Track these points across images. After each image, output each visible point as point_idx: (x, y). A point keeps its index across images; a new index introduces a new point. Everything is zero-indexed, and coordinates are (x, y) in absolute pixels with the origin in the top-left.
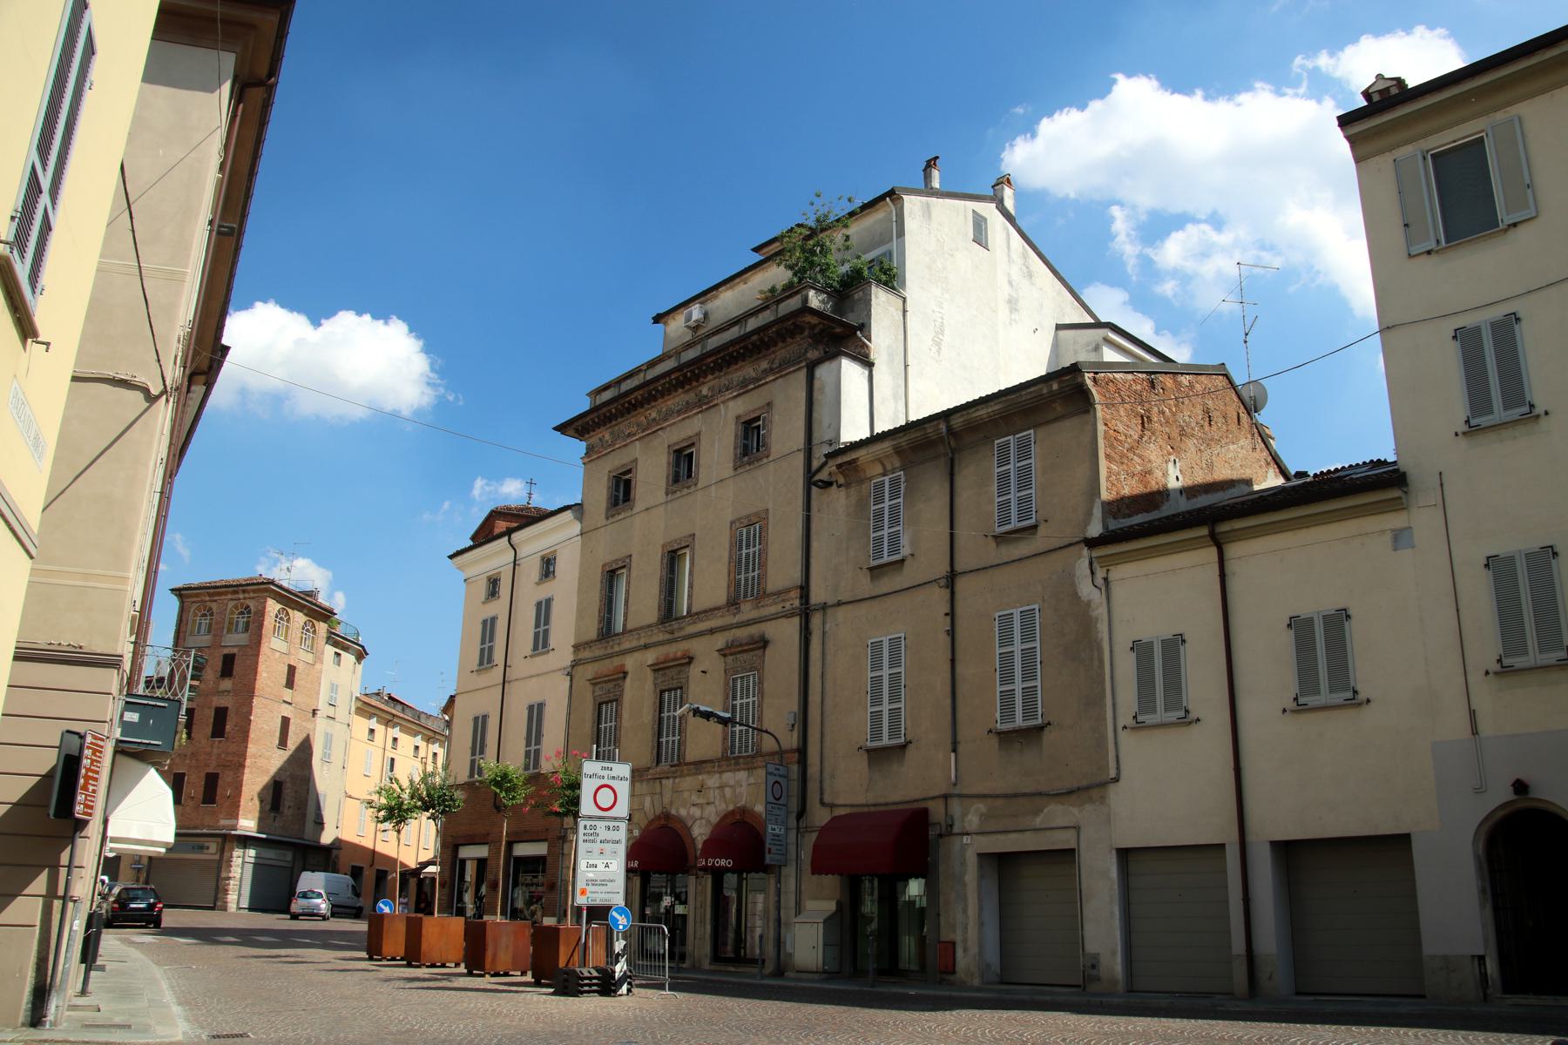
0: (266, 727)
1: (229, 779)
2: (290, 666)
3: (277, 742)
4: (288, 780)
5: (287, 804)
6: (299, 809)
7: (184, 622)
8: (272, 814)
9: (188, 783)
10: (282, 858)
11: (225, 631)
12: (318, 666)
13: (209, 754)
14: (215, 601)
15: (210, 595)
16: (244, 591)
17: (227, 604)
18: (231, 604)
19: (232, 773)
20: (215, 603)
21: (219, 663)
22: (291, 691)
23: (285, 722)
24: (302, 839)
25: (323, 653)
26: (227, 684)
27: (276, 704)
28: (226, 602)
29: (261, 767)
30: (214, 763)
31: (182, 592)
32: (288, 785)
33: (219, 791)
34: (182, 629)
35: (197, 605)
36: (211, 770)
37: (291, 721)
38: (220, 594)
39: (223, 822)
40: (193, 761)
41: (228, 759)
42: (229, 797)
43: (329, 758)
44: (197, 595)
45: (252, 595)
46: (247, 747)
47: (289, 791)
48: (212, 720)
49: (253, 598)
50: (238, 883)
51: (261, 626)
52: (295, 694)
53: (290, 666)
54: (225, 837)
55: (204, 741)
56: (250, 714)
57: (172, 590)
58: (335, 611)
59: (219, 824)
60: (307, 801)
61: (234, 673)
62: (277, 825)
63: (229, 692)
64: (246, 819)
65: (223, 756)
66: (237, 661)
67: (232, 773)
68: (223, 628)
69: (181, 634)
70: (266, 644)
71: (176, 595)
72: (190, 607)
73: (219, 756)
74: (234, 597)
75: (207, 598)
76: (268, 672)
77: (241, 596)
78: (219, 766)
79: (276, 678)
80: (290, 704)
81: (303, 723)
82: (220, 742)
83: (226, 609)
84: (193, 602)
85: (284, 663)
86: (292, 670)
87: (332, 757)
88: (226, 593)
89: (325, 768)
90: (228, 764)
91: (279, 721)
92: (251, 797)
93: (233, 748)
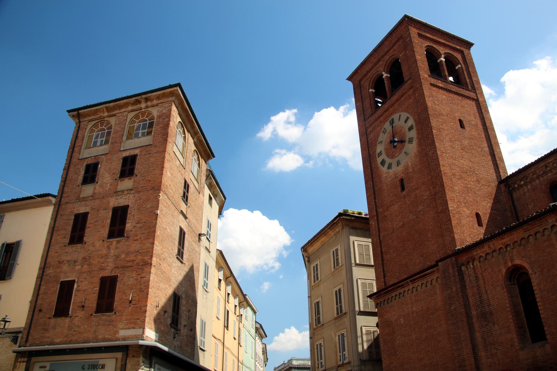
0: (168, 230)
1: (131, 281)
7: (79, 139)
9: (78, 290)
11: (125, 138)
14: (114, 115)
15: (108, 109)
16: (147, 100)
17: (127, 115)
19: (134, 274)
20: (114, 117)
21: (117, 166)
26: (127, 183)
27: (176, 212)
30: (111, 265)
31: (80, 112)
33: (118, 296)
34: (78, 144)
35: (93, 123)
36: (107, 273)
38: (120, 107)
39: (123, 333)
41: (128, 259)
42: (130, 302)
44: (96, 112)
45: (155, 102)
46: (154, 243)
49: (157, 105)
51: (167, 125)
54: (125, 349)
55: (98, 244)
56: (157, 208)
57: (69, 111)
59: (117, 336)
61: (136, 172)
65: (123, 256)
66: (137, 161)
68: (123, 135)
69: (76, 149)
71: (73, 116)
72: (87, 126)
73: (117, 257)
74: (134, 107)
75: (106, 114)
82: (118, 242)
83: (126, 120)
88: (126, 105)
90: (129, 264)
93: (135, 246)
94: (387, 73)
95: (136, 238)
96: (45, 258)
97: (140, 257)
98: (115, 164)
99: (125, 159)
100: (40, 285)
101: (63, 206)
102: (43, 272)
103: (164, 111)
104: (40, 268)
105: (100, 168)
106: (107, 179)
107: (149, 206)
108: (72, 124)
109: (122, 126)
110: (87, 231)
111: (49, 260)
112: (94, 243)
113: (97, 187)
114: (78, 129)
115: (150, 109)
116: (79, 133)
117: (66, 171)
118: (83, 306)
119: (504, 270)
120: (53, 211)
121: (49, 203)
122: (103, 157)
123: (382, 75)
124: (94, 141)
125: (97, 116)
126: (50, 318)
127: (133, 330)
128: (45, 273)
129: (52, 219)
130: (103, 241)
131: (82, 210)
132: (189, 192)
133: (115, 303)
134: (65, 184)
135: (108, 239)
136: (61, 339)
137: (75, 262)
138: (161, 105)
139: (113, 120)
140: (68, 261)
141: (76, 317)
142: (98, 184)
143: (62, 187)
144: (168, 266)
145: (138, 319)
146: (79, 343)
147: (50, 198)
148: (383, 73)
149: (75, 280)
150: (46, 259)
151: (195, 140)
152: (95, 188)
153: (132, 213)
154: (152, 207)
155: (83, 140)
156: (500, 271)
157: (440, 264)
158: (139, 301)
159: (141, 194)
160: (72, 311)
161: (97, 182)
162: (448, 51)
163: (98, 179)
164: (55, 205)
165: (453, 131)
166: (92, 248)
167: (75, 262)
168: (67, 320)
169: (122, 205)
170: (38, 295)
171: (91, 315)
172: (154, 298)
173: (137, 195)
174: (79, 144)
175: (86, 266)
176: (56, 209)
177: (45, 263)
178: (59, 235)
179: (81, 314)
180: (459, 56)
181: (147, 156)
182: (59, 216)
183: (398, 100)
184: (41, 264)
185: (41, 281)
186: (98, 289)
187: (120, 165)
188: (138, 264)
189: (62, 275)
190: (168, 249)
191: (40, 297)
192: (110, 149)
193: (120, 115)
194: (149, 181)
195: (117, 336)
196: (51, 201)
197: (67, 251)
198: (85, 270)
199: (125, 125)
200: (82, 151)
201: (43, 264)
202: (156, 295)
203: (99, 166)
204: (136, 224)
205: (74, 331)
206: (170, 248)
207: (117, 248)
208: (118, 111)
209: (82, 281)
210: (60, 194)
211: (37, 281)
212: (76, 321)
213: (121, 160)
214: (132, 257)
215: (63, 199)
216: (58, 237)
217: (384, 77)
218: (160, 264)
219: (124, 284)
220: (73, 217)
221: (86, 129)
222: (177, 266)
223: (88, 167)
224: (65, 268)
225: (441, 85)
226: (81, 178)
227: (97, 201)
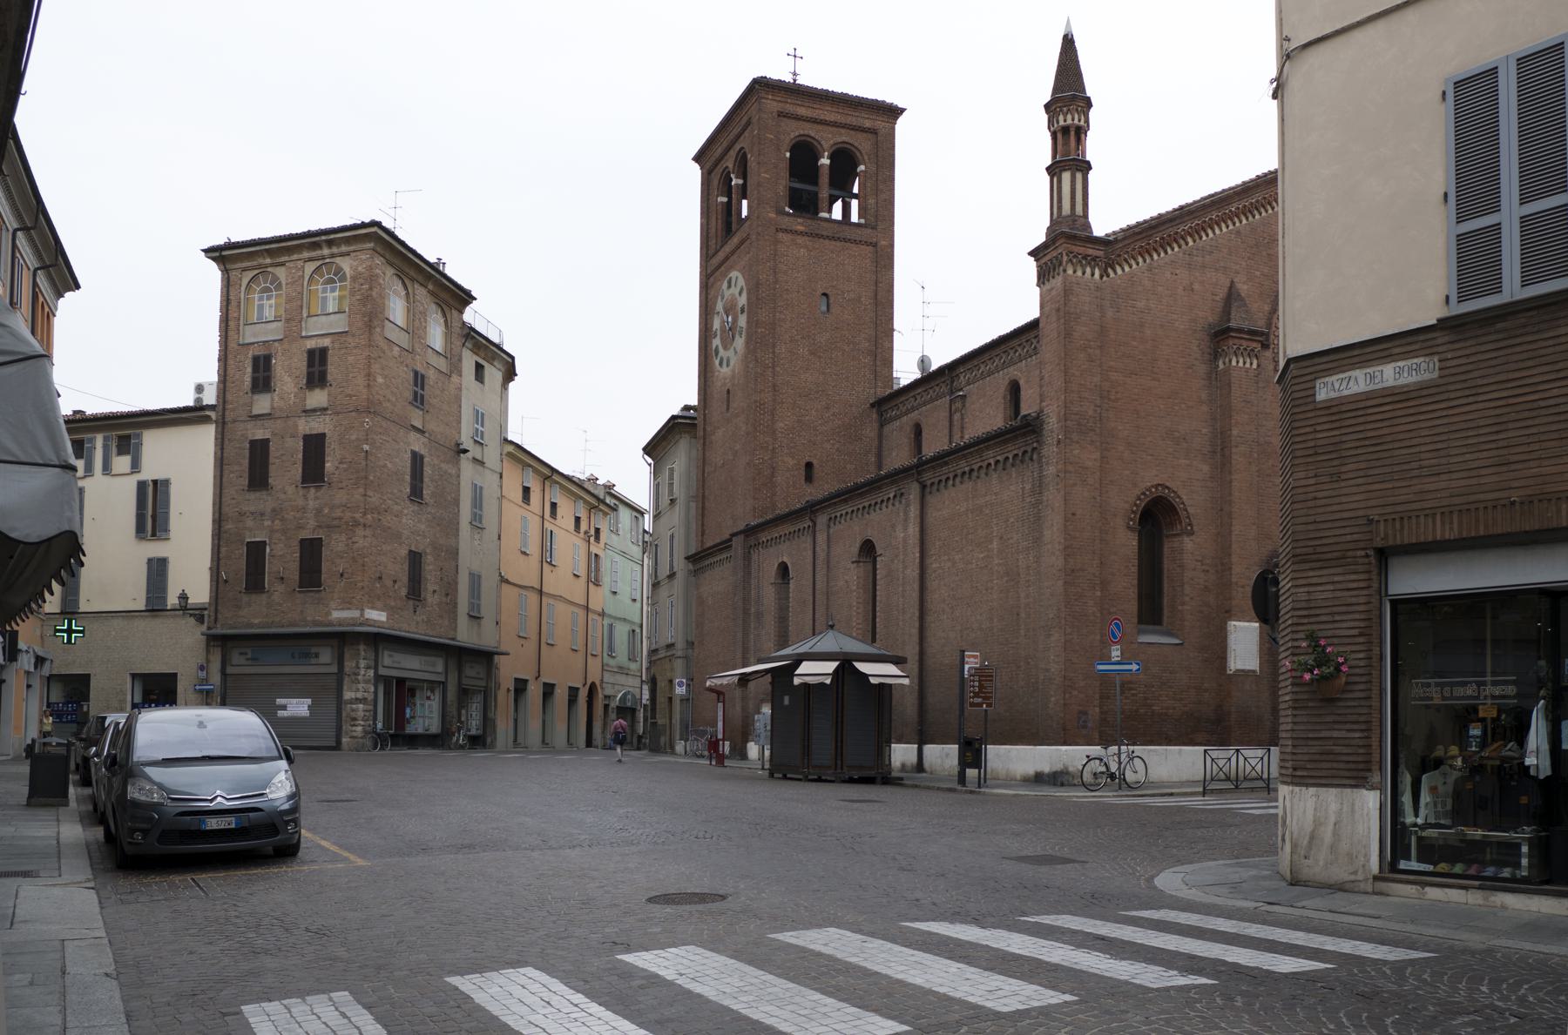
0: (389, 465)
1: (341, 547)
2: (416, 373)
3: (408, 490)
4: (428, 551)
5: (431, 588)
6: (447, 595)
7: (233, 304)
8: (411, 602)
10: (431, 669)
12: (455, 378)
13: (304, 509)
14: (282, 264)
17: (303, 267)
18: (310, 267)
19: (343, 537)
21: (301, 364)
22: (421, 413)
23: (417, 459)
24: (453, 639)
25: (460, 360)
26: (318, 398)
28: (300, 263)
29: (389, 528)
30: (312, 523)
32: (430, 558)
33: (325, 566)
34: (233, 314)
36: (306, 535)
37: (426, 460)
39: (337, 615)
40: (277, 522)
42: (342, 575)
43: (481, 522)
45: (344, 249)
47: (431, 567)
48: (300, 456)
50: (371, 707)
52: (428, 417)
53: (416, 373)
55: (291, 490)
57: (206, 251)
58: (473, 294)
59: (330, 618)
60: (456, 583)
61: (329, 377)
62: (419, 619)
63: (326, 409)
64: (372, 608)
66: (332, 359)
67: (343, 537)
68: (302, 307)
69: (232, 324)
70: (378, 330)
71: (214, 259)
72: (241, 279)
73: (319, 511)
76: (385, 377)
77: (326, 251)
78: (319, 527)
79: (397, 388)
80: (422, 432)
81: (443, 465)
83: (303, 276)
84: (245, 270)
85: (407, 366)
86: (419, 379)
87: (484, 522)
88: (299, 248)
89: (477, 536)
90: (336, 523)
91: (409, 455)
92: (378, 575)
94: (737, 178)
95: (340, 485)
96: (217, 506)
97: (349, 514)
98: (296, 360)
99: (311, 353)
100: (219, 546)
101: (230, 425)
102: (220, 527)
103: (360, 269)
104: (213, 521)
105: (275, 363)
106: (288, 385)
107: (353, 437)
108: (213, 272)
109: (299, 289)
110: (273, 470)
111: (225, 509)
112: (284, 487)
113: (276, 399)
114: (227, 285)
115: (338, 260)
116: (231, 293)
117: (222, 363)
118: (282, 578)
119: (776, 565)
120: (216, 432)
121: (207, 420)
122: (276, 344)
123: (731, 180)
124: (258, 305)
125: (255, 263)
126: (240, 592)
127: (348, 611)
128: (222, 529)
129: (216, 445)
130: (297, 486)
131: (260, 434)
132: (425, 388)
133: (323, 576)
134: (225, 387)
135: (302, 483)
136: (260, 620)
137: (262, 514)
138: (354, 254)
139: (281, 273)
140: (252, 513)
141: (274, 591)
142: (277, 392)
143: (222, 392)
144: (394, 518)
145: (353, 598)
146: (283, 626)
147: (208, 413)
148: (732, 176)
149: (265, 541)
150: (220, 508)
151: (430, 287)
152: (272, 400)
153: (332, 447)
154: (358, 439)
155: (239, 306)
156: (774, 565)
157: (734, 538)
158: (352, 574)
159: (341, 416)
160: (268, 584)
161: (275, 390)
162: (844, 137)
163: (275, 385)
164: (216, 422)
165: (803, 320)
166: (282, 496)
167: (262, 514)
168: (264, 596)
169: (315, 432)
170: (219, 559)
171: (294, 590)
172: (374, 569)
173: (336, 418)
174: (235, 315)
175: (277, 522)
176: (220, 429)
177: (220, 514)
178: (233, 472)
179: (280, 588)
180: (862, 144)
181: (343, 351)
182: (226, 442)
183: (738, 247)
184: (214, 515)
185: (219, 539)
186: (298, 555)
187: (305, 363)
188: (347, 523)
189: (248, 533)
190: (391, 493)
191: (222, 562)
192: (285, 331)
193: (291, 264)
194: (350, 396)
195: (330, 618)
196: (209, 417)
197: (247, 497)
198: (278, 528)
199: (303, 287)
200: (241, 328)
201: (217, 515)
202: (378, 562)
203: (274, 361)
204: (340, 463)
205: (275, 610)
206: (395, 491)
207: (317, 498)
208: (286, 258)
209: (275, 544)
210: (221, 400)
211: (213, 540)
212: (276, 597)
213: (306, 355)
214: (338, 513)
215: (227, 413)
216: (231, 475)
217: (733, 183)
218: (380, 520)
219: (332, 550)
220: (248, 445)
221: (241, 286)
222: (413, 511)
223: (256, 359)
224: (249, 523)
225: (800, 228)
226: (248, 379)
227: (279, 421)
